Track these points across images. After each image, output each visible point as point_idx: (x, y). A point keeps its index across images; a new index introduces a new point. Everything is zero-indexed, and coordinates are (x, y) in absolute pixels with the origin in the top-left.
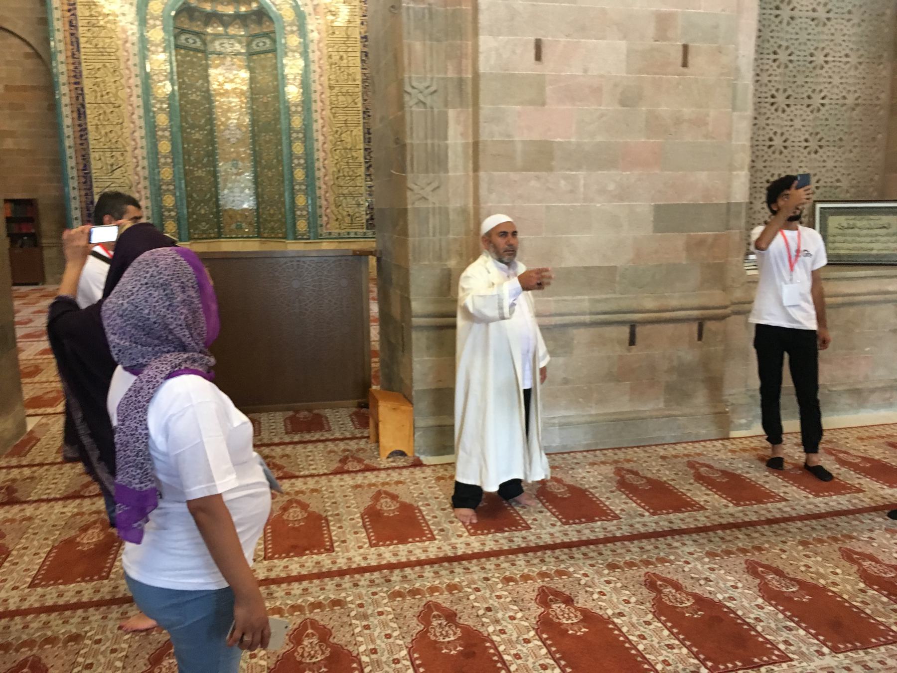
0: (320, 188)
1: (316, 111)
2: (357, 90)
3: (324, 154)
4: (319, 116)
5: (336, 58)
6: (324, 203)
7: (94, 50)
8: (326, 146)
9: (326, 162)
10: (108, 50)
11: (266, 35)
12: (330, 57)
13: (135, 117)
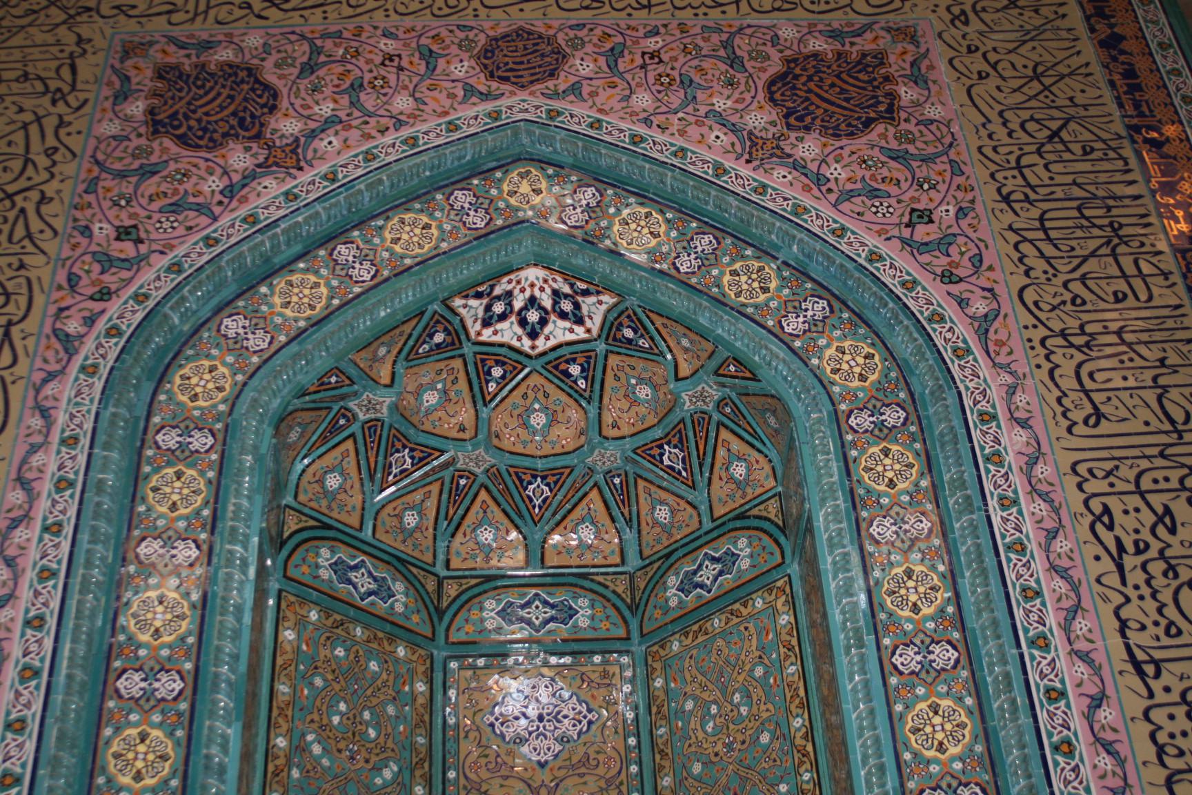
5: (1132, 521)
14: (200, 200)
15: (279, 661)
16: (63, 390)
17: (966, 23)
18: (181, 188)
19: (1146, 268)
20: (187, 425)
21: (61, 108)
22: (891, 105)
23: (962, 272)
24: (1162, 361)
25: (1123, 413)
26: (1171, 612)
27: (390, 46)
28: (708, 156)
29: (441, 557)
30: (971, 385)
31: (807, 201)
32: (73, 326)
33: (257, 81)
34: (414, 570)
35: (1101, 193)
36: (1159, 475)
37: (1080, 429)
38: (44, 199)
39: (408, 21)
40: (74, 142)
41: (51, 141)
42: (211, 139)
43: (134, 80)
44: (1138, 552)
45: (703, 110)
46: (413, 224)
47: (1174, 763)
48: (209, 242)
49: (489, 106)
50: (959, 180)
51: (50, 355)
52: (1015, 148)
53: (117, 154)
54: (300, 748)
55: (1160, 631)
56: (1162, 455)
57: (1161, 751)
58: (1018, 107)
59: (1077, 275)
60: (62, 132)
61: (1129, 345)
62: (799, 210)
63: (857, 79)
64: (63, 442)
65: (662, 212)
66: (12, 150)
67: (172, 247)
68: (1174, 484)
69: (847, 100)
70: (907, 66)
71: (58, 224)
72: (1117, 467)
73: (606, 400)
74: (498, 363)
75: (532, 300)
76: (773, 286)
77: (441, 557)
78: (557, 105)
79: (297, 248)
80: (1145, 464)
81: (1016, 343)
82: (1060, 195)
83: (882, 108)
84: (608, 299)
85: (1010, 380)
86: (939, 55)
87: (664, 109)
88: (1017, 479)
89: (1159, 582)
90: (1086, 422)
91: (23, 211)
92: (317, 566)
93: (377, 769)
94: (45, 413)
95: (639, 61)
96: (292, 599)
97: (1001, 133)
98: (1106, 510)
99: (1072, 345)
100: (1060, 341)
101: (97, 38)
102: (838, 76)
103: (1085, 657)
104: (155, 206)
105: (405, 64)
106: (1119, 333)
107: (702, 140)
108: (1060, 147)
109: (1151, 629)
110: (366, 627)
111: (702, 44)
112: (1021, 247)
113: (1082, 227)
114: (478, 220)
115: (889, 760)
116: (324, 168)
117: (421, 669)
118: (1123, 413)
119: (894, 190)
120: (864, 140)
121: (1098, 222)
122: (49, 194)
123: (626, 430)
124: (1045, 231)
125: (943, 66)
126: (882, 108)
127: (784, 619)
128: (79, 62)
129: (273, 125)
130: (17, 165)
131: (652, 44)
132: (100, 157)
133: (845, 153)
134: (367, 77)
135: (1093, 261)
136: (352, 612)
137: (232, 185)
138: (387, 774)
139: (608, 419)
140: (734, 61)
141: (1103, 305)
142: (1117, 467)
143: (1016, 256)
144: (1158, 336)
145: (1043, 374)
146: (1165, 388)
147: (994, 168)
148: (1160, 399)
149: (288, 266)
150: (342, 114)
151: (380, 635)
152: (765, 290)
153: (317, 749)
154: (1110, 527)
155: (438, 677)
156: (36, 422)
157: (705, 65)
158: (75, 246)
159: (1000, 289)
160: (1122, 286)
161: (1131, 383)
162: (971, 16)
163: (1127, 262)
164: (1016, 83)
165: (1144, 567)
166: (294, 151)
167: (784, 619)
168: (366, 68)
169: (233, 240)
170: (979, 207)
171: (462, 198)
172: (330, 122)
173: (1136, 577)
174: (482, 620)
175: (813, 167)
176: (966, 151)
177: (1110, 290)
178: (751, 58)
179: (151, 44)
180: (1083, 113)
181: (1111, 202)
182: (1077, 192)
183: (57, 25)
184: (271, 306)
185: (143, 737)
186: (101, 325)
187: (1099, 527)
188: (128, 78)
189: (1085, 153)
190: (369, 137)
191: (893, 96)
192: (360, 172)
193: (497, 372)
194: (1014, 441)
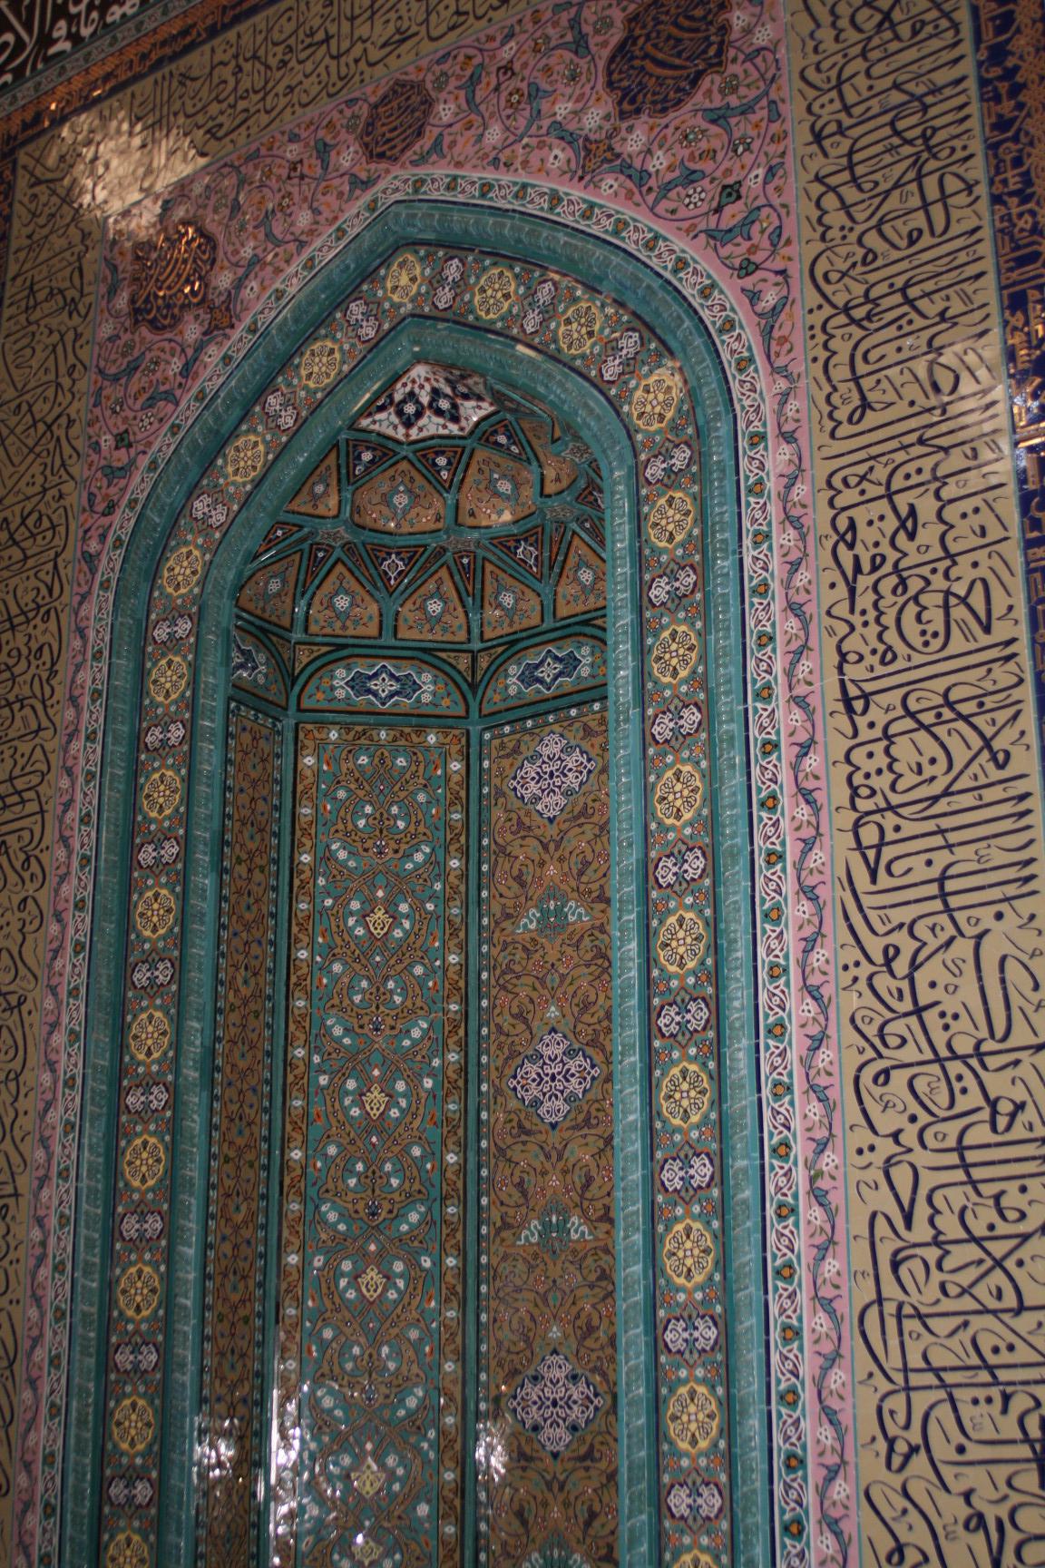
0: (792, 1333)
2: (1003, 676)
3: (815, 1109)
4: (789, 887)
6: (815, 1434)
8: (825, 1057)
9: (829, 1160)
12: (848, 535)
13: (60, 1039)
14: (166, 387)
15: (300, 788)
16: (90, 609)
19: (952, 184)
21: (76, 320)
22: (722, 43)
24: (942, 314)
26: (891, 637)
27: (292, 151)
28: (546, 185)
29: (476, 631)
30: (747, 403)
31: (628, 213)
32: (93, 546)
34: (443, 655)
35: (921, 90)
36: (911, 468)
38: (71, 422)
39: (312, 112)
41: (72, 360)
42: (173, 316)
44: (874, 569)
45: (546, 123)
47: (864, 805)
48: (175, 429)
49: (367, 197)
50: (775, 127)
52: (838, 58)
54: (329, 857)
56: (921, 441)
59: (873, 222)
61: (910, 302)
63: (691, 18)
65: (512, 268)
68: (926, 476)
72: (871, 469)
73: (542, 458)
74: (438, 454)
77: (476, 631)
78: (421, 172)
80: (900, 457)
81: (798, 338)
82: (876, 110)
83: (712, 52)
85: (783, 384)
87: (512, 138)
90: (850, 420)
92: (332, 688)
93: (409, 856)
95: (494, 83)
96: (310, 727)
99: (853, 321)
100: (842, 319)
102: (676, 24)
103: (800, 702)
105: (306, 171)
106: (903, 290)
108: (888, 35)
110: (390, 726)
112: (824, 203)
117: (454, 749)
119: (707, 166)
120: (689, 107)
121: (909, 135)
122: (73, 416)
126: (712, 52)
131: (506, 53)
136: (372, 719)
138: (419, 857)
141: (896, 255)
142: (871, 469)
143: (815, 214)
144: (945, 280)
147: (811, 93)
149: (234, 433)
151: (407, 730)
153: (342, 855)
154: (851, 546)
155: (474, 750)
157: (552, 61)
160: (919, 220)
163: (931, 184)
166: (228, 309)
174: (506, 688)
175: (637, 164)
177: (904, 231)
181: (929, 100)
182: (897, 97)
187: (842, 547)
188: (115, 267)
189: (915, 33)
194: (778, 458)
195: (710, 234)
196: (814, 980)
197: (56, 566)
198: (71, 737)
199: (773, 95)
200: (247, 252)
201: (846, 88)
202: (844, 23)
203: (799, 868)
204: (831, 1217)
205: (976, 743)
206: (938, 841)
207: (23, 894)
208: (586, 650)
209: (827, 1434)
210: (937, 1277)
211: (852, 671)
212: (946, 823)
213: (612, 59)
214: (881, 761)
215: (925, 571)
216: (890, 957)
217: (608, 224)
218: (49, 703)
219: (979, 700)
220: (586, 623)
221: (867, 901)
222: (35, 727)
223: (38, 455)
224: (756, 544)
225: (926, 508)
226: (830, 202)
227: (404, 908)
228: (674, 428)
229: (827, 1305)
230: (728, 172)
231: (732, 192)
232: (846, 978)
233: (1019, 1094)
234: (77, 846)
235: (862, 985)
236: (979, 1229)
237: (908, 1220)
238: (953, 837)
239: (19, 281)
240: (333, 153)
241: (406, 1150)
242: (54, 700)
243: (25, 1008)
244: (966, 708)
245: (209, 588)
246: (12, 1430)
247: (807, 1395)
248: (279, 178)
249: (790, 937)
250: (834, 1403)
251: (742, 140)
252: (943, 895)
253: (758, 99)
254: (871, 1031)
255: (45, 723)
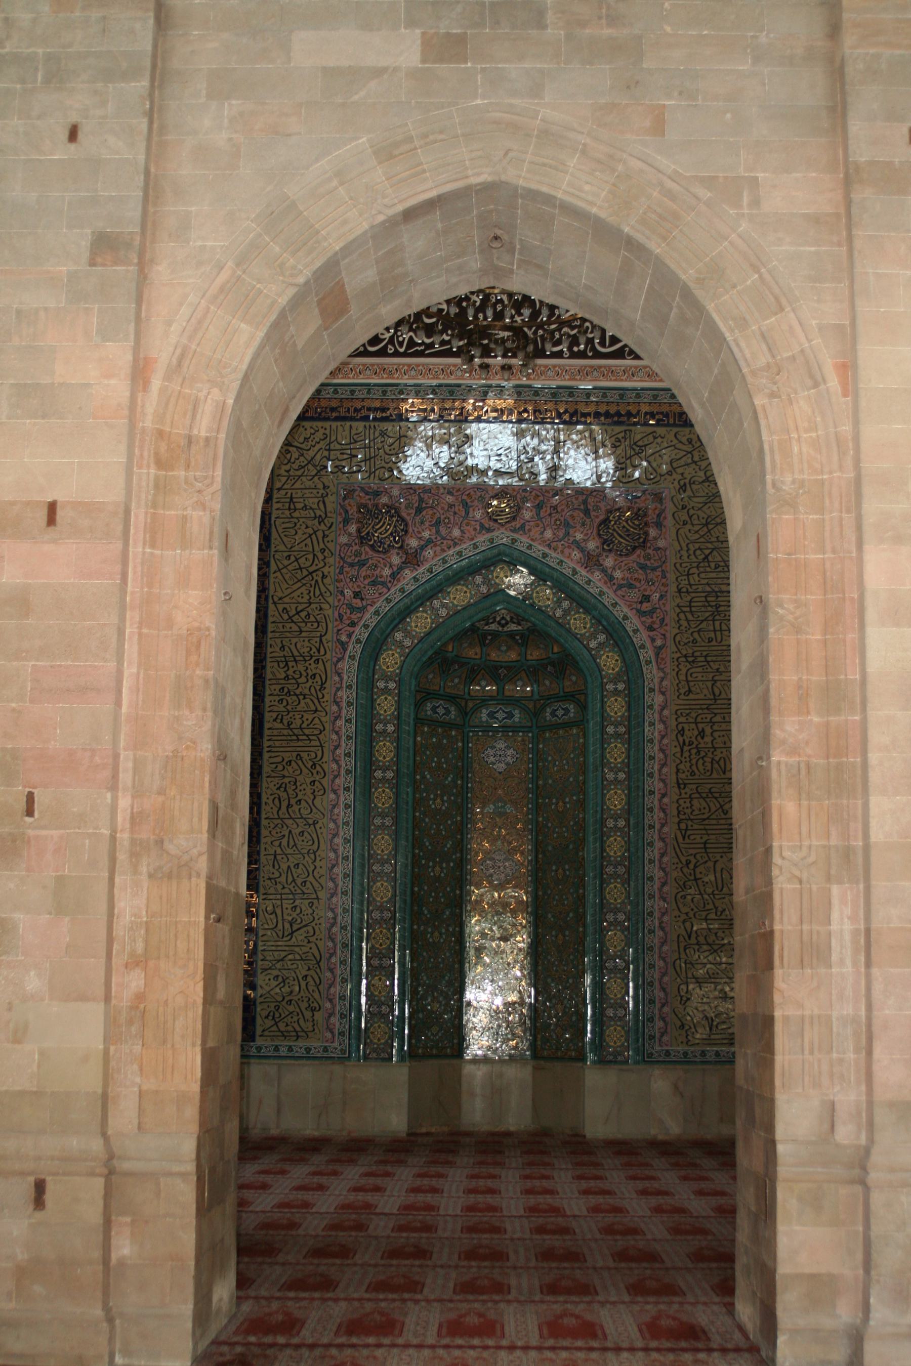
0: (652, 966)
1: (651, 827)
4: (656, 837)
5: (691, 733)
7: (285, 732)
8: (665, 889)
9: (666, 918)
10: (307, 732)
11: (570, 697)
14: (382, 580)
16: (344, 665)
17: (685, 491)
18: (375, 573)
20: (387, 678)
21: (323, 527)
22: (645, 539)
23: (655, 626)
24: (718, 669)
25: (698, 691)
26: (694, 768)
28: (572, 565)
31: (605, 589)
32: (344, 638)
33: (399, 516)
35: (716, 589)
36: (704, 716)
37: (682, 697)
38: (324, 577)
40: (331, 546)
41: (322, 546)
43: (350, 513)
44: (690, 745)
45: (572, 539)
46: (461, 591)
47: (682, 817)
48: (388, 601)
50: (664, 580)
51: (337, 650)
53: (349, 554)
54: (424, 777)
55: (689, 774)
56: (707, 708)
57: (679, 812)
58: (694, 542)
60: (326, 540)
61: (708, 662)
62: (602, 593)
64: (347, 687)
66: (307, 549)
67: (375, 603)
68: (708, 720)
69: (628, 535)
70: (655, 516)
71: (331, 588)
75: (503, 618)
76: (588, 626)
78: (516, 536)
79: (419, 603)
80: (700, 711)
82: (700, 590)
83: (641, 540)
84: (529, 624)
85: (662, 675)
86: (670, 508)
88: (656, 716)
89: (693, 756)
91: (317, 581)
93: (447, 778)
94: (339, 675)
95: (548, 512)
97: (685, 558)
98: (683, 729)
99: (687, 661)
100: (684, 659)
101: (331, 485)
104: (366, 582)
105: (457, 511)
106: (706, 656)
107: (569, 557)
108: (706, 564)
109: (686, 773)
110: (441, 727)
111: (575, 502)
113: (704, 606)
114: (484, 589)
115: (599, 809)
116: (427, 566)
118: (698, 691)
119: (638, 585)
120: (631, 558)
122: (326, 573)
123: (535, 657)
124: (690, 607)
125: (670, 517)
127: (581, 740)
128: (326, 499)
129: (406, 542)
130: (310, 557)
132: (343, 555)
133: (623, 564)
134: (442, 517)
135: (705, 623)
137: (393, 573)
138: (449, 779)
139: (529, 652)
140: (587, 512)
145: (674, 673)
146: (715, 681)
148: (713, 685)
149: (416, 610)
150: (433, 537)
152: (585, 628)
153: (428, 776)
154: (682, 735)
156: (337, 678)
158: (339, 600)
159: (668, 635)
160: (712, 635)
161: (704, 679)
162: (688, 485)
163: (717, 623)
164: (697, 528)
165: (690, 751)
166: (416, 556)
167: (581, 740)
168: (442, 512)
169: (397, 600)
170: (668, 594)
171: (479, 579)
172: (429, 541)
173: (686, 754)
175: (609, 571)
176: (669, 566)
178: (594, 510)
179: (354, 491)
180: (721, 546)
181: (719, 594)
183: (314, 476)
184: (411, 627)
185: (384, 791)
186: (354, 638)
188: (347, 512)
189: (716, 568)
190: (443, 551)
191: (646, 534)
192: (441, 569)
193: (489, 637)
194: (659, 699)
195: (638, 611)
196: (664, 866)
197: (321, 640)
198: (336, 718)
199: (664, 568)
200: (426, 534)
201: (690, 577)
202: (691, 552)
203: (660, 831)
204: (666, 934)
205: (718, 806)
206: (704, 832)
207: (313, 779)
208: (517, 712)
209: (662, 994)
210: (697, 954)
211: (681, 776)
212: (707, 827)
213: (600, 525)
214: (689, 805)
215: (706, 750)
216: (688, 863)
217: (597, 591)
218: (322, 700)
219: (720, 793)
220: (518, 701)
221: (682, 845)
222: (314, 709)
223: (304, 585)
224: (650, 726)
225: (708, 731)
226: (682, 616)
227: (445, 798)
228: (618, 674)
229: (664, 959)
230: (645, 590)
231: (647, 598)
232: (674, 867)
233: (724, 907)
234: (344, 765)
235: (679, 870)
236: (710, 941)
237: (690, 937)
238: (709, 832)
239: (283, 492)
240: (471, 509)
241: (446, 888)
242: (325, 699)
243: (317, 826)
244: (717, 795)
245: (404, 671)
246: (321, 987)
247: (656, 984)
248: (443, 508)
249: (656, 851)
250: (665, 986)
251: (651, 580)
252: (705, 848)
253: (658, 567)
254: (681, 883)
255: (319, 708)
